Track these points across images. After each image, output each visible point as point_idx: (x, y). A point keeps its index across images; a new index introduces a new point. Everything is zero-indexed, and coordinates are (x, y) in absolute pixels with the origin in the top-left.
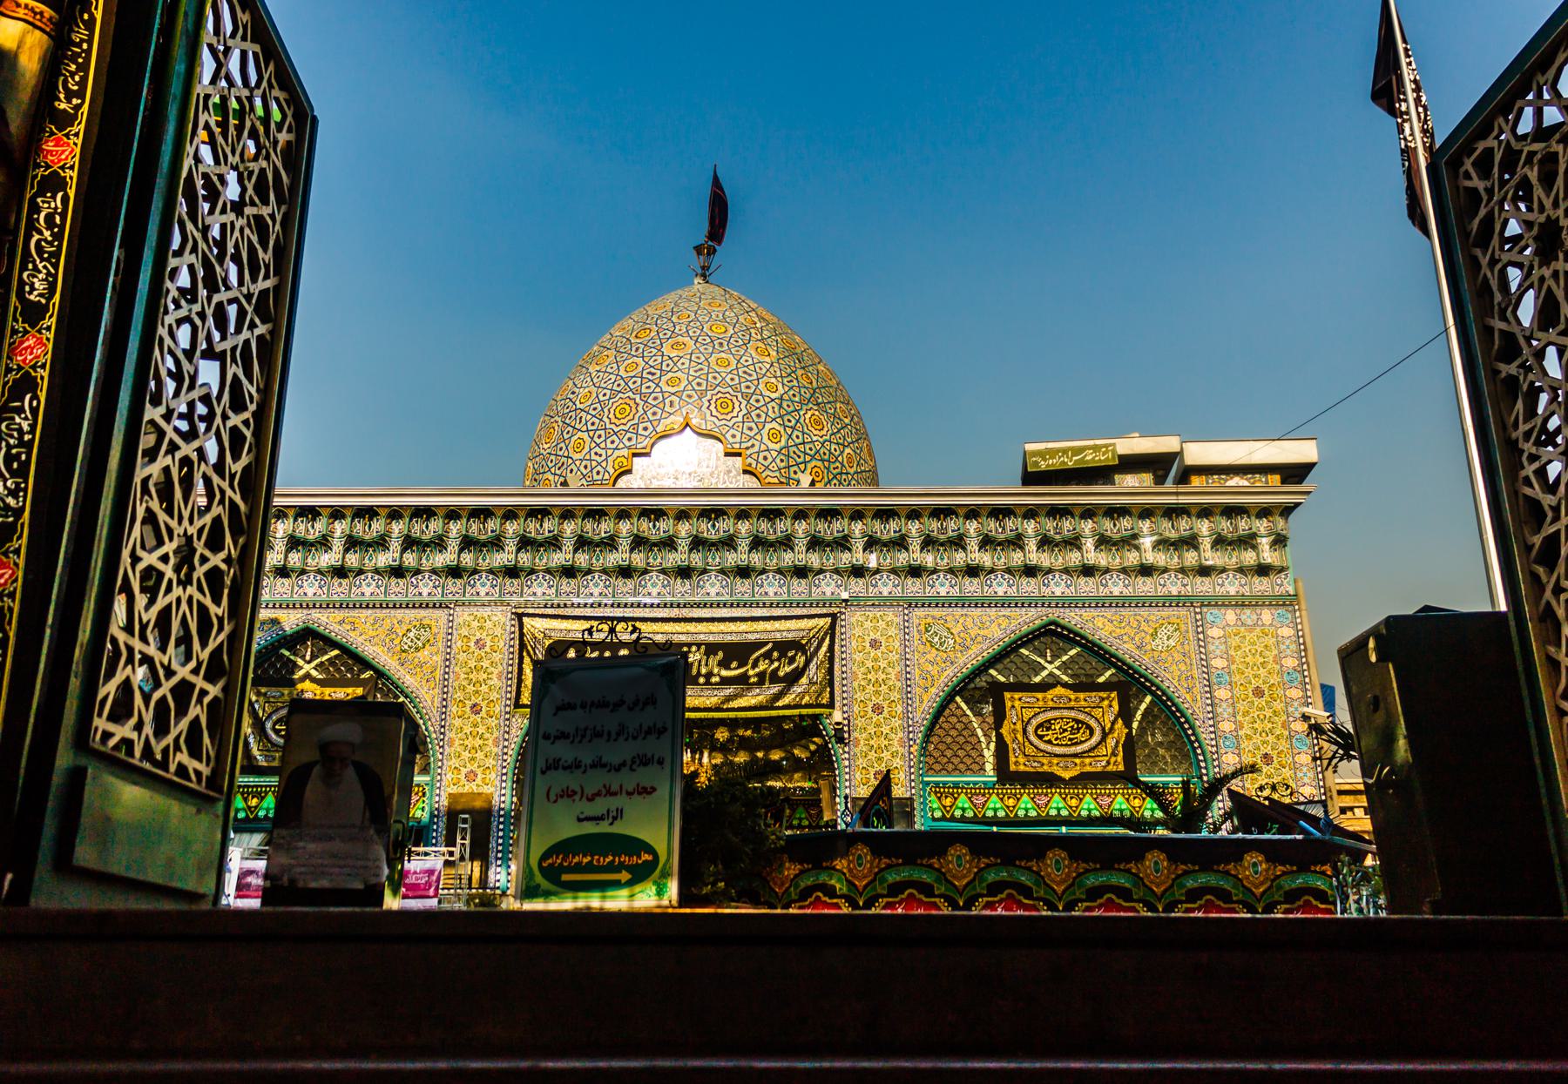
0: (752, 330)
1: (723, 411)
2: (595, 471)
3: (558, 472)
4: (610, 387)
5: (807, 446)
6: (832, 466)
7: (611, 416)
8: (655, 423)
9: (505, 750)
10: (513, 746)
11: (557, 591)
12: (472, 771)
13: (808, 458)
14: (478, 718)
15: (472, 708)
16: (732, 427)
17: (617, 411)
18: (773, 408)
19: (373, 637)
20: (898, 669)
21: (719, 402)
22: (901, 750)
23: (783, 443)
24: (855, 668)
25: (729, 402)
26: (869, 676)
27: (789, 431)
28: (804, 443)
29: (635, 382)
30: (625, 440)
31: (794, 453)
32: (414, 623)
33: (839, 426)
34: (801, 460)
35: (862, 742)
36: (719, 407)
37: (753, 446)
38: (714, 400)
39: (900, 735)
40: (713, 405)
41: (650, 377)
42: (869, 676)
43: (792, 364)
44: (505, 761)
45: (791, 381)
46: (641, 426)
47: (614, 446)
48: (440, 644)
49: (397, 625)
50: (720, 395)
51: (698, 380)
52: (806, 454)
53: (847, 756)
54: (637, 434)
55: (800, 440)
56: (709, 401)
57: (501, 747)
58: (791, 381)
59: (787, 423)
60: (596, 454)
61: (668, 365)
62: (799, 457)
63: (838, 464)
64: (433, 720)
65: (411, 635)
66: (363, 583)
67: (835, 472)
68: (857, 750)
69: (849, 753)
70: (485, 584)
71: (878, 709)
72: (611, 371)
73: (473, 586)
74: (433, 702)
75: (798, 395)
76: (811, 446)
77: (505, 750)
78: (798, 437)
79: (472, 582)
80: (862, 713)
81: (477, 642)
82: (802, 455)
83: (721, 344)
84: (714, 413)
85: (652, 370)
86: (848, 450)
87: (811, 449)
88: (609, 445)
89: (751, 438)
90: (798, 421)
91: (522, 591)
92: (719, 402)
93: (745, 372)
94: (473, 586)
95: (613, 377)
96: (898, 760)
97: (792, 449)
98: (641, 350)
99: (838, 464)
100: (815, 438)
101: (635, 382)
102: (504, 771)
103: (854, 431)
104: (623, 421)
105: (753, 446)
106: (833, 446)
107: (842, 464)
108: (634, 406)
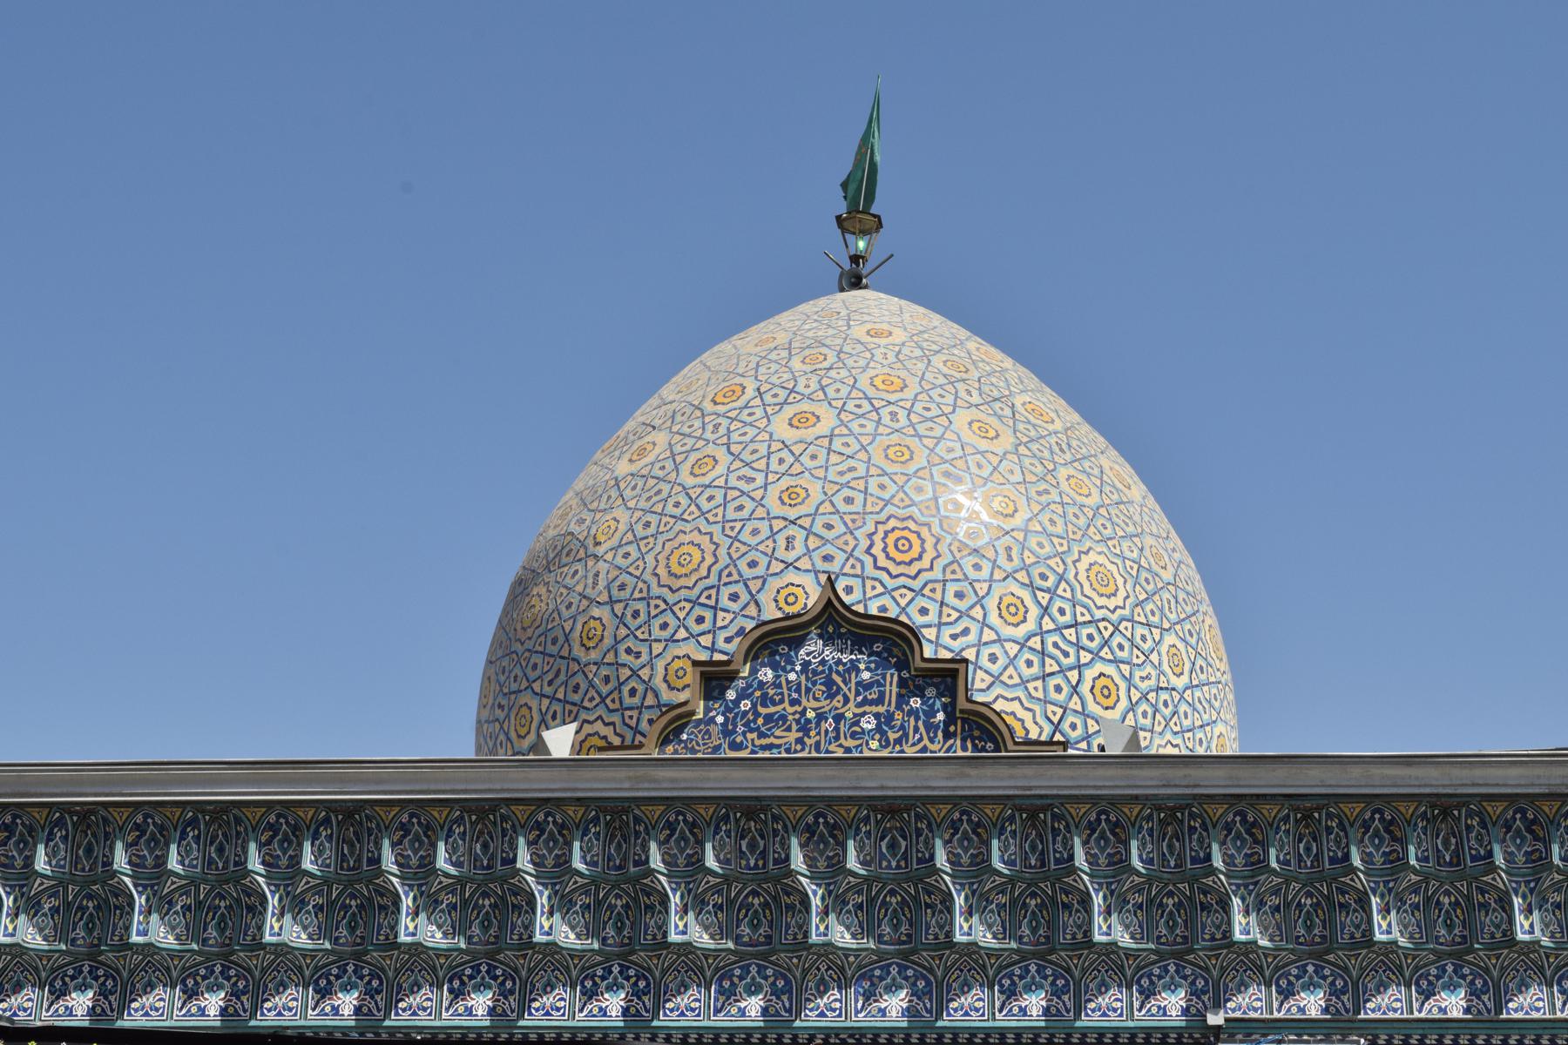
0: (960, 386)
1: (899, 557)
2: (626, 690)
3: (548, 690)
4: (658, 508)
5: (1085, 631)
6: (1138, 674)
7: (661, 571)
8: (754, 586)
13: (1085, 657)
16: (920, 592)
17: (674, 559)
18: (1009, 549)
21: (891, 540)
23: (1030, 625)
25: (913, 537)
27: (1044, 598)
28: (1075, 625)
29: (711, 498)
30: (691, 622)
31: (1056, 645)
33: (1150, 588)
34: (1072, 660)
36: (891, 549)
37: (966, 632)
38: (881, 534)
40: (879, 546)
41: (742, 485)
43: (1046, 454)
45: (1047, 492)
46: (725, 592)
47: (666, 634)
50: (892, 523)
51: (846, 492)
52: (1079, 647)
54: (715, 608)
55: (1067, 619)
56: (870, 536)
58: (1047, 492)
59: (1039, 582)
60: (629, 651)
61: (781, 461)
62: (1066, 654)
63: (1149, 669)
67: (1144, 686)
72: (661, 474)
75: (1060, 521)
76: (1091, 630)
78: (1062, 612)
82: (1072, 651)
83: (893, 415)
84: (882, 562)
85: (747, 471)
86: (1170, 639)
87: (1090, 637)
88: (657, 632)
89: (962, 614)
90: (1061, 578)
92: (891, 540)
93: (947, 474)
95: (666, 488)
97: (1050, 639)
98: (722, 430)
99: (1149, 669)
100: (1099, 614)
101: (711, 498)
103: (1181, 595)
104: (682, 582)
105: (966, 632)
106: (1140, 631)
107: (1158, 667)
108: (710, 548)
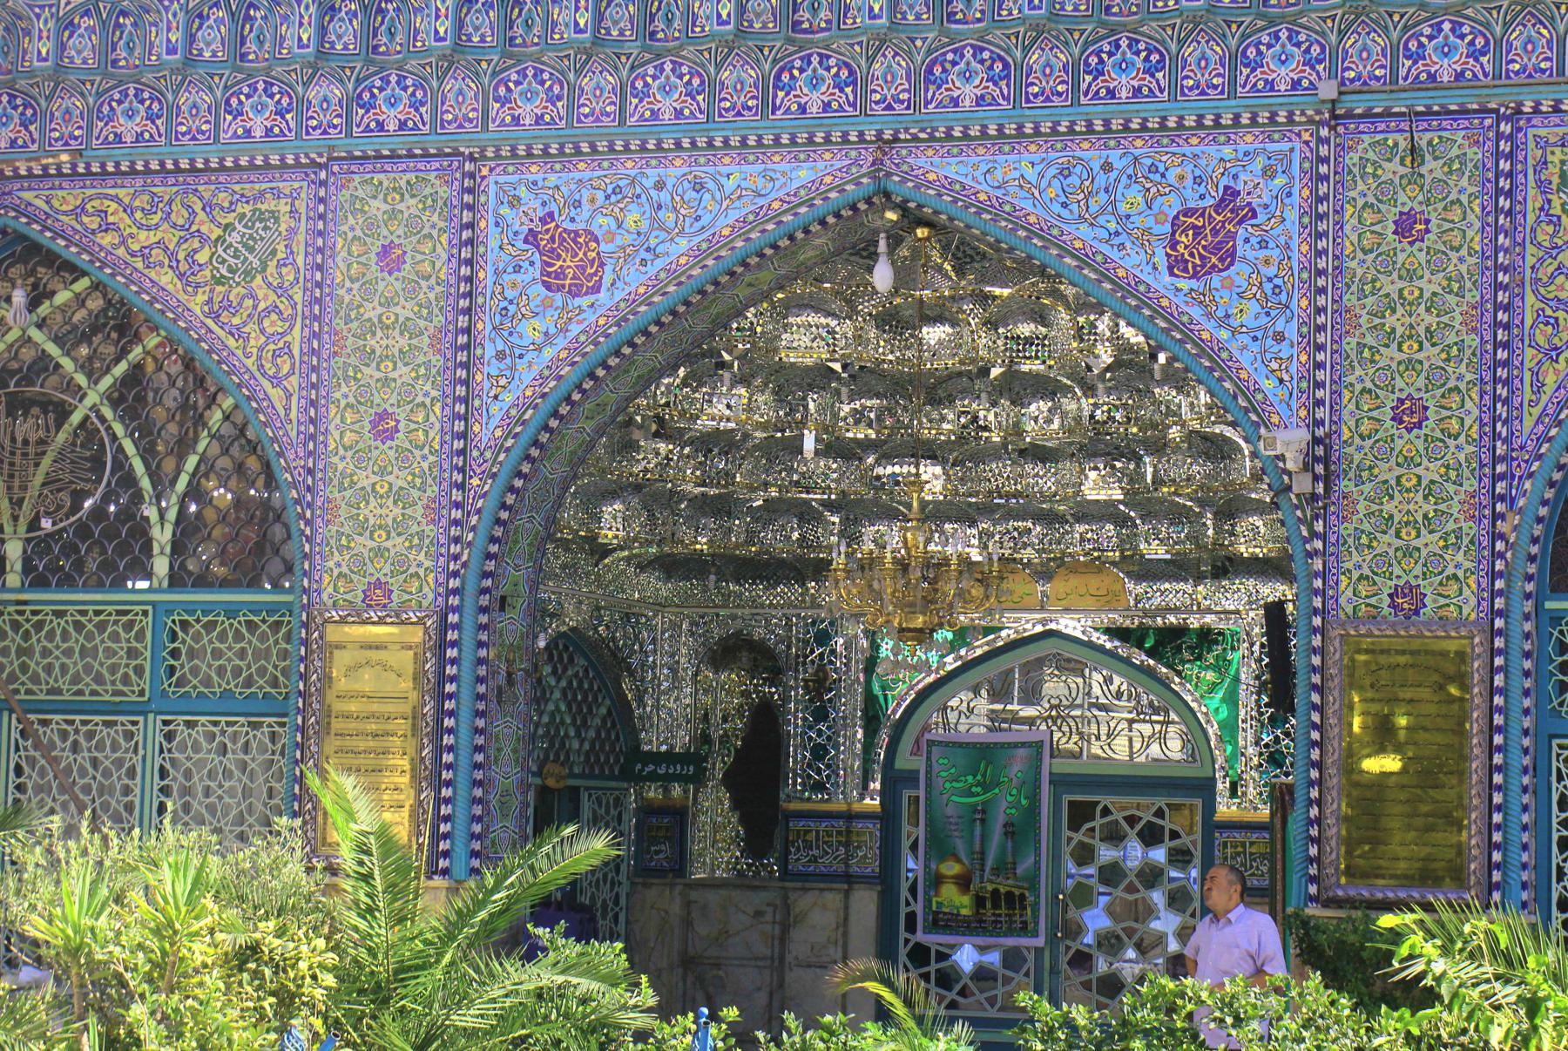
9: (455, 532)
10: (474, 520)
11: (570, 108)
12: (379, 584)
14: (387, 451)
15: (374, 424)
19: (151, 247)
20: (1472, 296)
22: (1469, 528)
24: (1350, 299)
26: (1390, 321)
32: (239, 209)
35: (1361, 507)
39: (1470, 485)
42: (1390, 321)
44: (456, 558)
48: (300, 260)
49: (202, 215)
53: (1319, 544)
57: (444, 522)
64: (290, 455)
65: (233, 238)
66: (119, 110)
68: (1347, 529)
69: (1323, 537)
70: (398, 100)
71: (1409, 414)
73: (368, 107)
74: (287, 409)
77: (455, 532)
79: (366, 96)
80: (1365, 427)
81: (386, 250)
91: (486, 112)
94: (368, 107)
96: (1460, 557)
102: (454, 583)
